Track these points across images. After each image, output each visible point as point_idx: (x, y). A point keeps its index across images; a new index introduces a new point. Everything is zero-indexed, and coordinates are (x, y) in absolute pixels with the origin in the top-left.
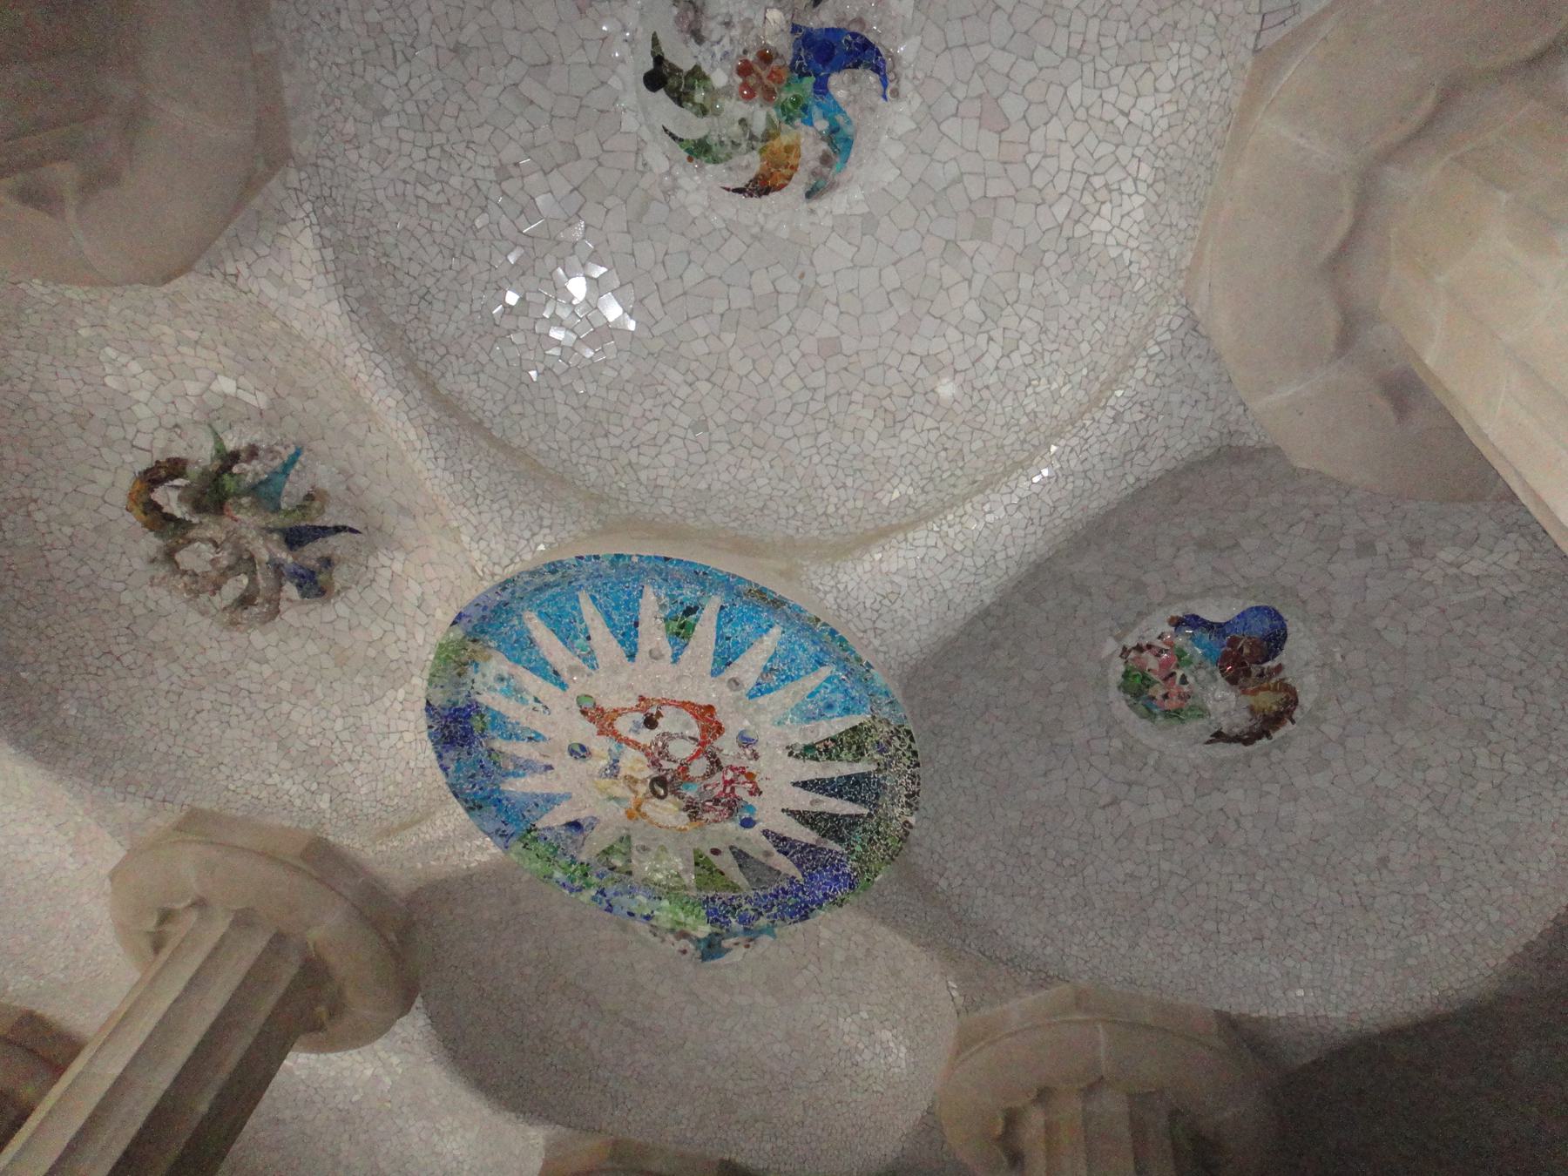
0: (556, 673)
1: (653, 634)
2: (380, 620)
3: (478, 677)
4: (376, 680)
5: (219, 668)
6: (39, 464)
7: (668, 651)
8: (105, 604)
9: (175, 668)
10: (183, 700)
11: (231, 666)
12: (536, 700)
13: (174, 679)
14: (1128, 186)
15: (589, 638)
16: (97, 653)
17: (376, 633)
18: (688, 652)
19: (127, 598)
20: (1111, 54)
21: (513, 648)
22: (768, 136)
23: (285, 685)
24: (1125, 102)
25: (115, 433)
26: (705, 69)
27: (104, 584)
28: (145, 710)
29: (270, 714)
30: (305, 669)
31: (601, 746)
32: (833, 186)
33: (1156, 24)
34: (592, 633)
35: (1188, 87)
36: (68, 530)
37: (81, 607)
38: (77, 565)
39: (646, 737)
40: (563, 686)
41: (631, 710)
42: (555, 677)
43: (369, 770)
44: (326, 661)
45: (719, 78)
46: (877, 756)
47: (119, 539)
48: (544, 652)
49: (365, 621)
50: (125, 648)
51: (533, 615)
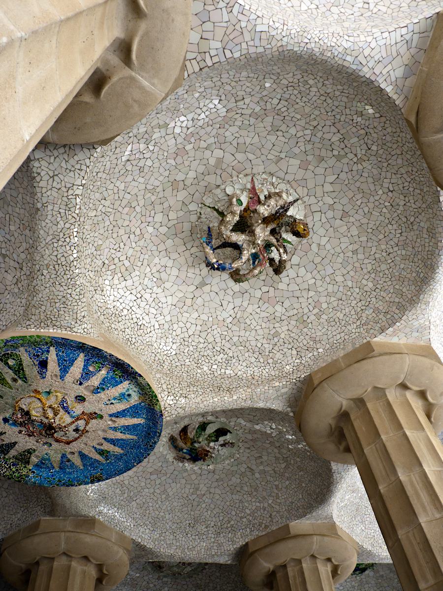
0: (118, 417)
1: (107, 446)
2: (176, 222)
3: (135, 389)
4: (153, 198)
5: (227, 126)
6: (358, 184)
7: (98, 447)
8: (302, 123)
9: (249, 112)
10: (233, 100)
11: (221, 131)
12: (112, 403)
13: (245, 107)
14: (122, 498)
15: (121, 432)
16: (293, 97)
17: (172, 215)
18: (94, 451)
19: (293, 131)
20: (148, 501)
21: (136, 409)
22: (192, 444)
23: (189, 147)
24: (138, 501)
25: (330, 214)
26: (216, 443)
27: (308, 132)
28: (248, 85)
29: (185, 130)
30: (187, 163)
31: (78, 409)
32: (170, 440)
33: (148, 512)
34: (122, 434)
35: (132, 516)
36: (335, 153)
37: (313, 116)
38: (324, 136)
39: (73, 427)
40: (111, 415)
41: (85, 427)
42: (118, 415)
43: (117, 170)
44: (180, 177)
45: (212, 444)
46: (11, 461)
47: (310, 158)
48: (128, 418)
49: (181, 213)
50: (280, 106)
51: (142, 422)
